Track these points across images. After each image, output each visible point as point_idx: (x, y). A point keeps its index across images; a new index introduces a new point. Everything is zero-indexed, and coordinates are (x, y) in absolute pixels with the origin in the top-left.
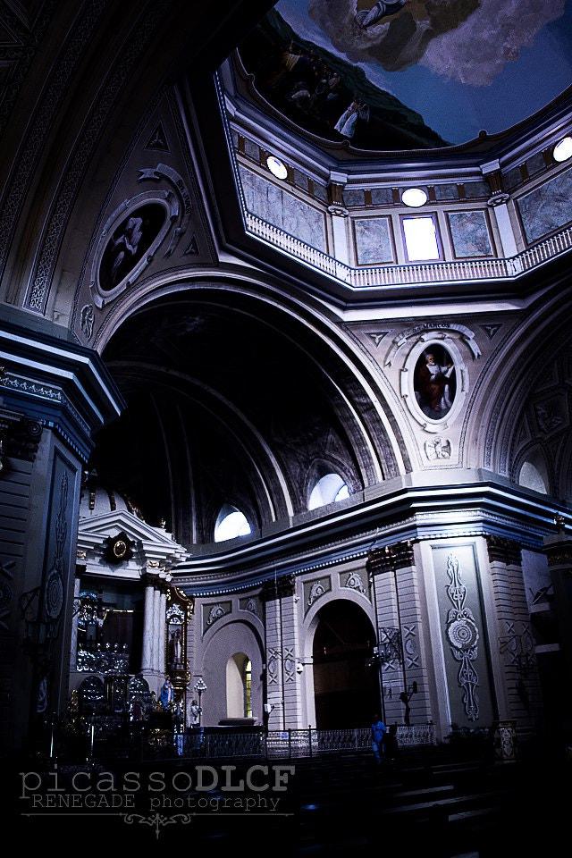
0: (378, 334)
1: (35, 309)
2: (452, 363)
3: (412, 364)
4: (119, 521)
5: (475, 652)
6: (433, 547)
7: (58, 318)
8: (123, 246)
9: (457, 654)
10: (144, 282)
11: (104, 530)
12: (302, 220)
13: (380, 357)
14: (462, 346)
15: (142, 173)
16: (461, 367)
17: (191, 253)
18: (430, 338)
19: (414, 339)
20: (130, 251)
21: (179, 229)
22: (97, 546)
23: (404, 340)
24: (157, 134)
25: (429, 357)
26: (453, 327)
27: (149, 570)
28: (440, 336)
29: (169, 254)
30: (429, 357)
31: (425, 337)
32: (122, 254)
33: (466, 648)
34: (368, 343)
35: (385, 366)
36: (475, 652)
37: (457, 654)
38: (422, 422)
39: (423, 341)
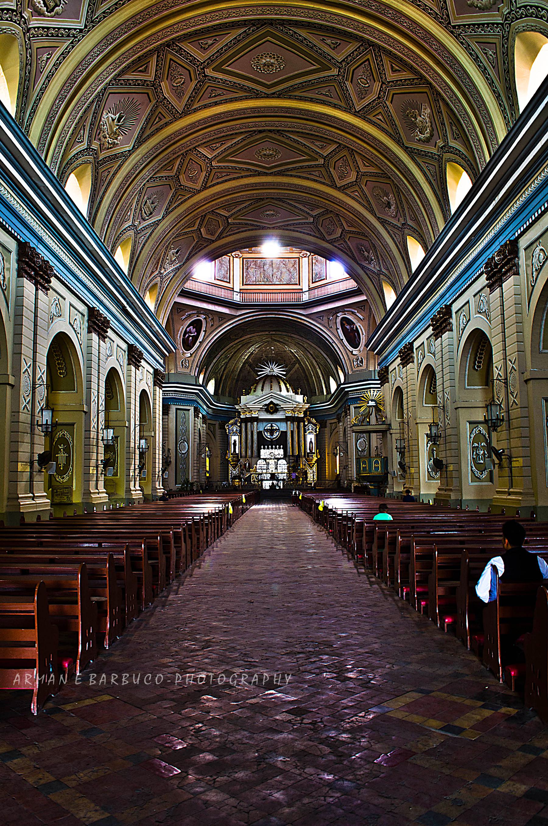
2: (353, 323)
3: (339, 326)
5: (366, 452)
6: (355, 408)
8: (190, 336)
9: (359, 453)
10: (208, 337)
12: (284, 270)
13: (327, 325)
14: (355, 316)
16: (358, 325)
18: (340, 315)
19: (335, 316)
22: (261, 408)
25: (344, 322)
26: (346, 309)
29: (212, 325)
30: (344, 322)
32: (191, 338)
33: (363, 451)
34: (320, 321)
36: (366, 452)
37: (359, 453)
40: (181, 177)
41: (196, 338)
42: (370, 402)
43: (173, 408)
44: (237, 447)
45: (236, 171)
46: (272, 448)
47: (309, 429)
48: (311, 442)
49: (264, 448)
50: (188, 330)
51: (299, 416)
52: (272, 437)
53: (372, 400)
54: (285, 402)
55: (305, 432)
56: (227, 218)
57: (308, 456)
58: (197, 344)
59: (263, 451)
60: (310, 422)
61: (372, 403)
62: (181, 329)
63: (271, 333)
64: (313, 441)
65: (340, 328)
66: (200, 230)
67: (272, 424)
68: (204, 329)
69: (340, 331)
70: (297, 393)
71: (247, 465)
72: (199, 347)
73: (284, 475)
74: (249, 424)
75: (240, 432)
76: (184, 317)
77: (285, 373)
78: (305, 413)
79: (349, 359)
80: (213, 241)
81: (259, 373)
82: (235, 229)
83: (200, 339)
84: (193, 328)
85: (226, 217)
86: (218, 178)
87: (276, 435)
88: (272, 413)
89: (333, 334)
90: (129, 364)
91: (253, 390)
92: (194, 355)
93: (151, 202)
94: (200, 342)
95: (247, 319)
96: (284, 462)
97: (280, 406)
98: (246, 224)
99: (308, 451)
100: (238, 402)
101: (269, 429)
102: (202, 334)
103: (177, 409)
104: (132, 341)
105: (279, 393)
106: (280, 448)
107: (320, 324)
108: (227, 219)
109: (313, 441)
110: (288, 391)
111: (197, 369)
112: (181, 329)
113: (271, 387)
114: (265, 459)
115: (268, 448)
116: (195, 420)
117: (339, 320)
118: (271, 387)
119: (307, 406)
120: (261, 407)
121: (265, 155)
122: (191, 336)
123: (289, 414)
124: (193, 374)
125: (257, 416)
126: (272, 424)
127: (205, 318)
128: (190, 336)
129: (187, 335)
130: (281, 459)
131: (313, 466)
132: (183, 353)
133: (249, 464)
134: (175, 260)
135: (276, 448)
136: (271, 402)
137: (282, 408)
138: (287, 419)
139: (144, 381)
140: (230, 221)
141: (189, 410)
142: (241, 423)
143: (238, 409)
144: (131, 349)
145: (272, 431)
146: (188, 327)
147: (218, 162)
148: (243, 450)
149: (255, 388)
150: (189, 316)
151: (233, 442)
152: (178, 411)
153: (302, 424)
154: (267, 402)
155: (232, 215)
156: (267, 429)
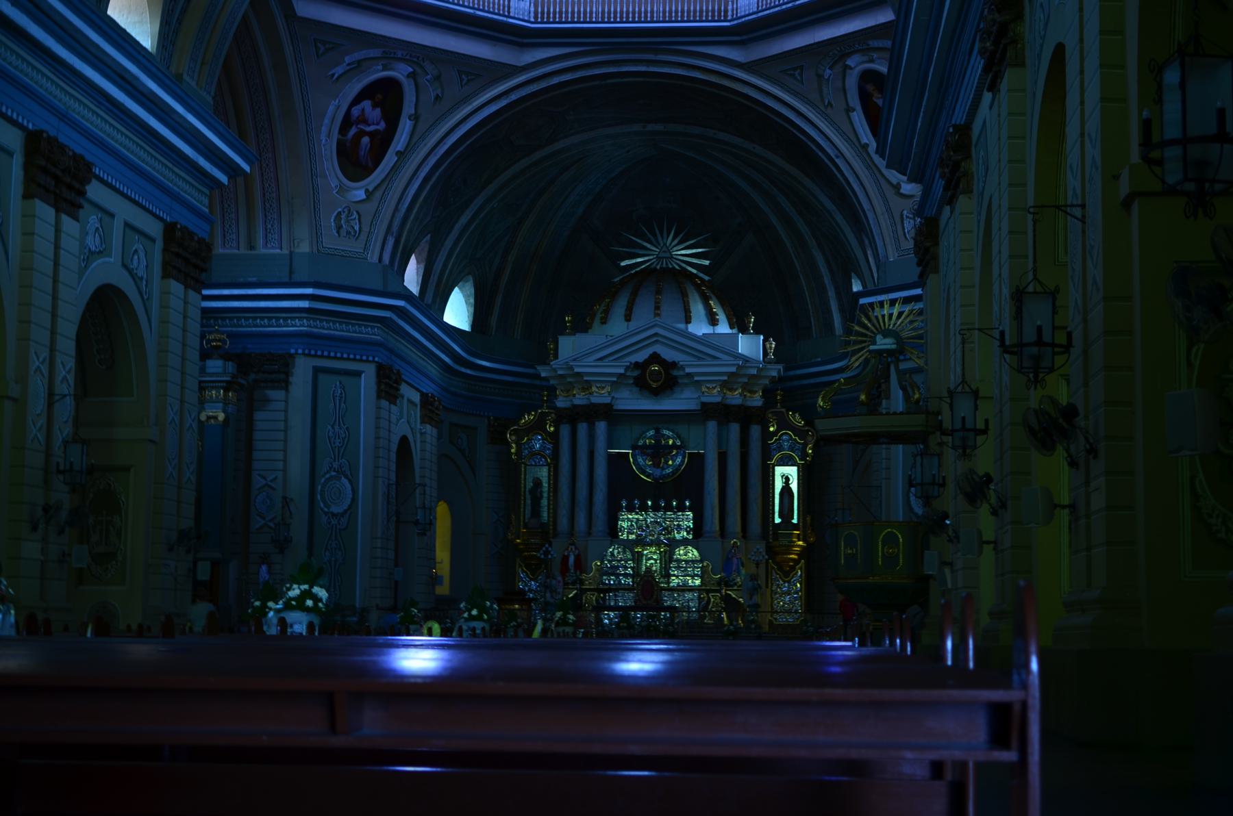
0: (795, 69)
1: (273, 248)
3: (854, 100)
4: (656, 334)
7: (298, 246)
8: (362, 133)
11: (637, 350)
15: (334, 75)
17: (468, 81)
18: (857, 63)
20: (377, 131)
21: (429, 77)
23: (828, 71)
24: (319, 45)
25: (870, 88)
27: (704, 399)
28: (865, 58)
29: (437, 97)
30: (870, 88)
31: (850, 62)
32: (366, 140)
35: (826, 107)
38: (894, 182)
39: (851, 68)
41: (382, 142)
42: (879, 338)
43: (302, 370)
44: (544, 502)
46: (656, 508)
47: (780, 448)
48: (786, 489)
49: (631, 509)
50: (356, 111)
51: (749, 403)
52: (658, 472)
53: (886, 333)
54: (700, 356)
55: (766, 454)
57: (776, 537)
58: (390, 159)
59: (626, 521)
60: (783, 424)
61: (884, 343)
62: (331, 108)
63: (650, 127)
64: (794, 486)
65: (859, 108)
67: (658, 431)
68: (408, 108)
69: (859, 118)
70: (744, 330)
71: (572, 559)
72: (395, 169)
73: (688, 596)
74: (582, 428)
75: (556, 455)
76: (339, 70)
77: (707, 263)
78: (768, 393)
79: (889, 210)
81: (623, 264)
83: (400, 140)
84: (375, 106)
87: (676, 462)
88: (656, 393)
89: (838, 129)
90: (27, 196)
91: (599, 316)
92: (378, 195)
94: (399, 154)
95: (556, 80)
96: (693, 553)
97: (683, 368)
99: (778, 520)
100: (545, 354)
101: (650, 446)
102: (405, 126)
103: (317, 371)
104: (37, 120)
105: (682, 326)
106: (681, 508)
107: (795, 94)
109: (794, 486)
110: (713, 321)
111: (391, 242)
112: (331, 108)
113: (657, 308)
114: (628, 545)
115: (644, 508)
116: (379, 408)
117: (852, 82)
118: (657, 308)
119: (774, 371)
120: (622, 371)
122: (370, 134)
123: (714, 396)
124: (376, 259)
125: (607, 400)
126: (658, 431)
127: (412, 75)
128: (362, 133)
129: (353, 131)
130: (685, 542)
131: (793, 568)
132: (342, 190)
133: (578, 558)
135: (668, 508)
136: (655, 358)
137: (689, 375)
138: (707, 412)
139: (114, 259)
141: (358, 374)
142: (557, 424)
143: (546, 379)
144: (36, 143)
145: (658, 452)
146: (357, 100)
148: (563, 513)
149: (607, 312)
150: (358, 67)
151: (530, 485)
152: (321, 376)
153: (755, 431)
154: (641, 357)
156: (645, 446)
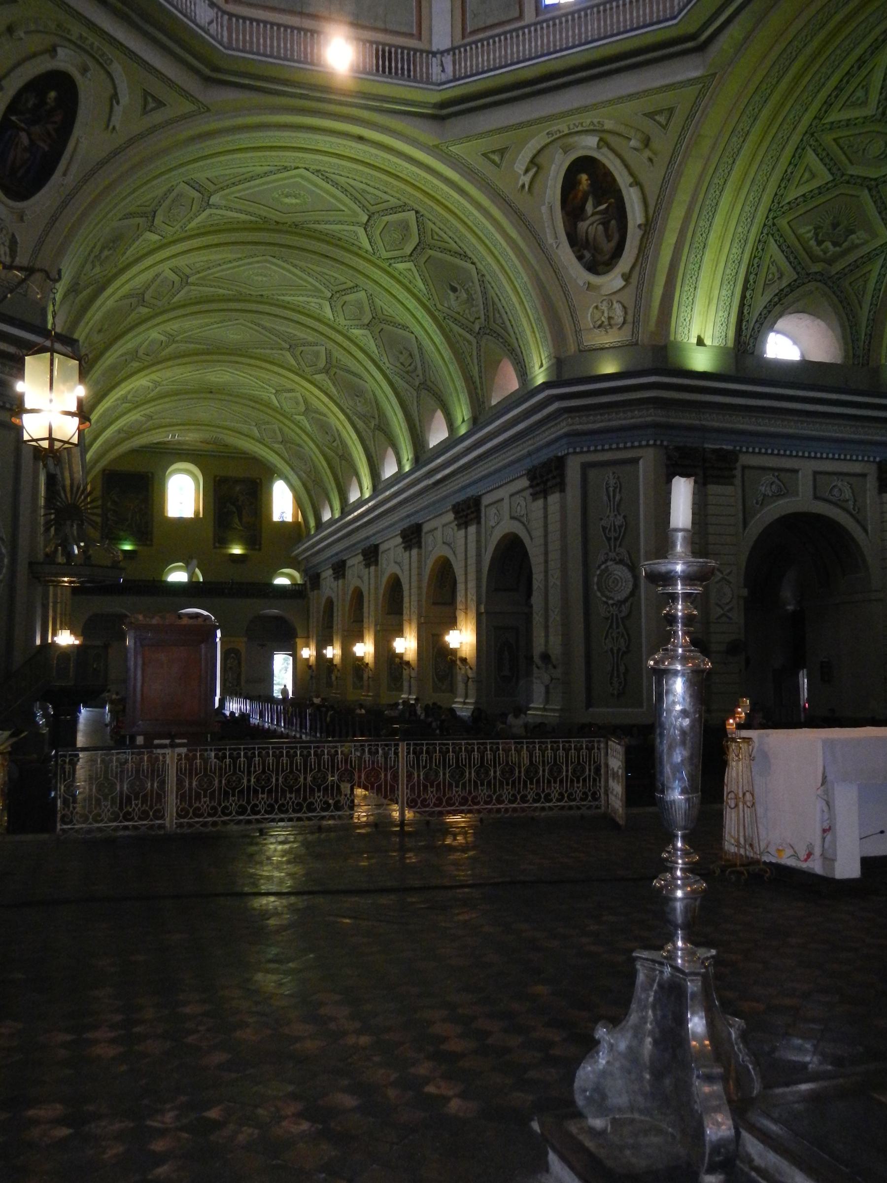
40: (366, 321)
45: (310, 271)
56: (366, 226)
66: (411, 255)
80: (417, 212)
82: (368, 197)
85: (365, 229)
86: (336, 279)
93: (400, 356)
98: (345, 191)
108: (366, 224)
121: (265, 276)
134: (467, 291)
140: (365, 218)
147: (323, 292)
155: (353, 224)
